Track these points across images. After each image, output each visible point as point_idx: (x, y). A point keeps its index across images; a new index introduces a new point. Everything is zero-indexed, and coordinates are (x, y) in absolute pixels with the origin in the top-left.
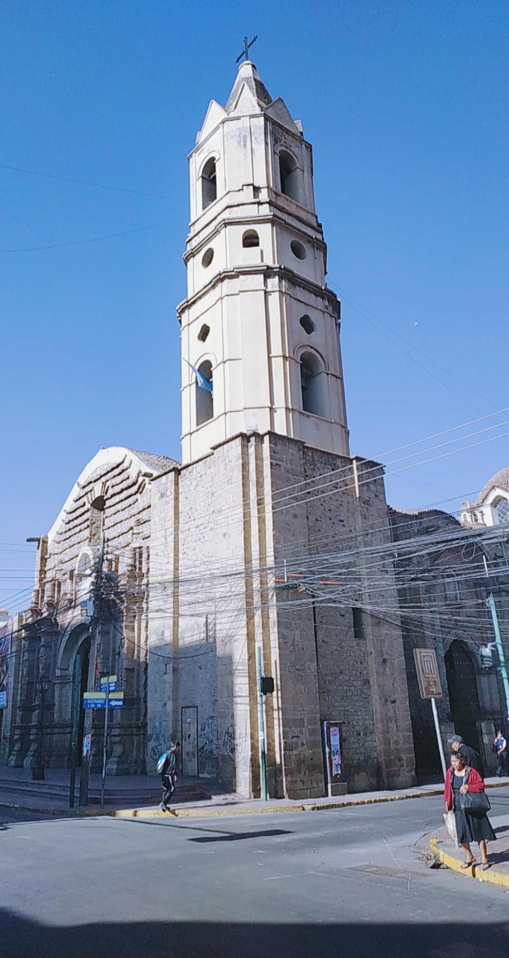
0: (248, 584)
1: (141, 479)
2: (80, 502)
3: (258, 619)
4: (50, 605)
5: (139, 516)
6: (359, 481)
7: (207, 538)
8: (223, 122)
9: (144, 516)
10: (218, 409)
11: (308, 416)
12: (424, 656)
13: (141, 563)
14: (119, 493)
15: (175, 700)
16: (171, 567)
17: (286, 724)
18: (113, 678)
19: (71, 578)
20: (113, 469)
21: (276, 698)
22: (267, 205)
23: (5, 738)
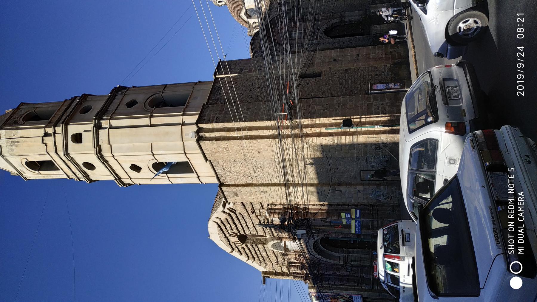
0: (288, 136)
1: (226, 210)
3: (308, 131)
4: (302, 267)
5: (250, 212)
6: (228, 74)
7: (261, 165)
9: (249, 208)
10: (183, 159)
11: (188, 103)
14: (236, 226)
15: (357, 185)
17: (370, 113)
18: (343, 215)
19: (287, 255)
20: (222, 230)
21: (356, 120)
22: (56, 128)
23: (380, 295)
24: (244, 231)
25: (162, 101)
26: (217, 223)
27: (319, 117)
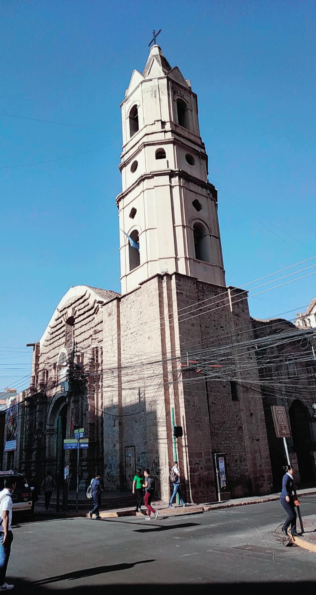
0: (165, 368)
1: (96, 305)
2: (59, 321)
3: (171, 390)
4: (42, 385)
5: (95, 328)
6: (232, 301)
7: (137, 341)
8: (141, 83)
9: (98, 328)
10: (143, 260)
11: (199, 262)
12: (278, 411)
13: (97, 357)
15: (121, 443)
16: (116, 359)
17: (191, 455)
18: (82, 430)
19: (55, 368)
22: (170, 133)
24: (77, 323)
25: (201, 236)
26: (85, 295)
27: (186, 401)
